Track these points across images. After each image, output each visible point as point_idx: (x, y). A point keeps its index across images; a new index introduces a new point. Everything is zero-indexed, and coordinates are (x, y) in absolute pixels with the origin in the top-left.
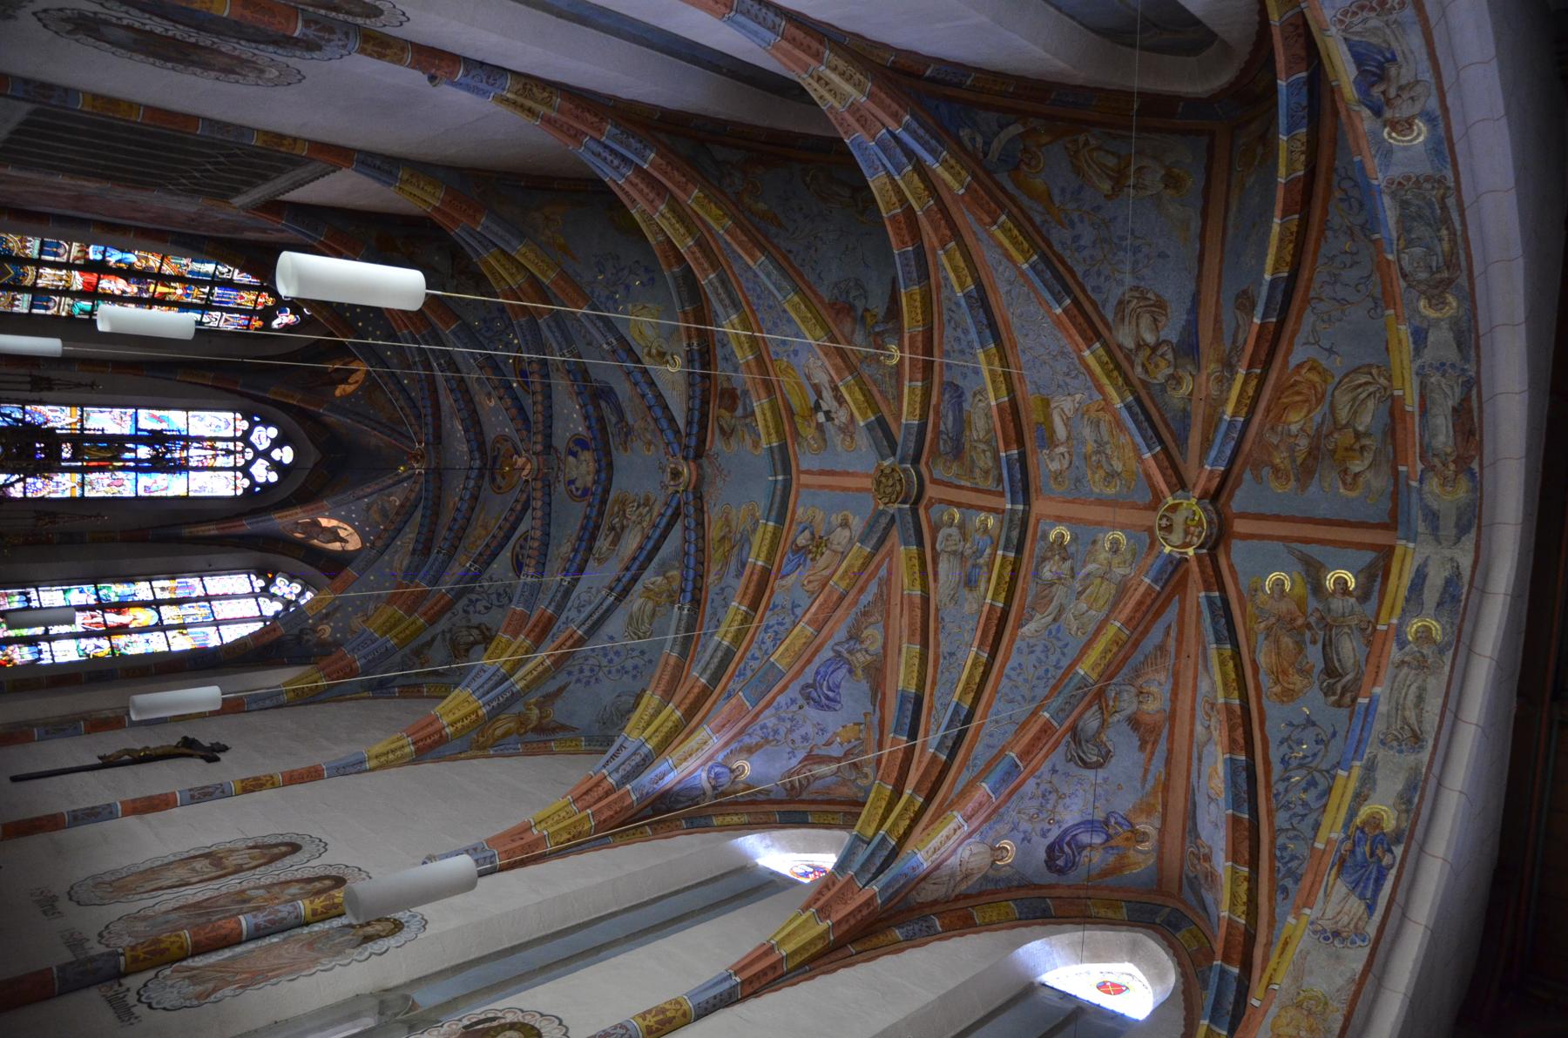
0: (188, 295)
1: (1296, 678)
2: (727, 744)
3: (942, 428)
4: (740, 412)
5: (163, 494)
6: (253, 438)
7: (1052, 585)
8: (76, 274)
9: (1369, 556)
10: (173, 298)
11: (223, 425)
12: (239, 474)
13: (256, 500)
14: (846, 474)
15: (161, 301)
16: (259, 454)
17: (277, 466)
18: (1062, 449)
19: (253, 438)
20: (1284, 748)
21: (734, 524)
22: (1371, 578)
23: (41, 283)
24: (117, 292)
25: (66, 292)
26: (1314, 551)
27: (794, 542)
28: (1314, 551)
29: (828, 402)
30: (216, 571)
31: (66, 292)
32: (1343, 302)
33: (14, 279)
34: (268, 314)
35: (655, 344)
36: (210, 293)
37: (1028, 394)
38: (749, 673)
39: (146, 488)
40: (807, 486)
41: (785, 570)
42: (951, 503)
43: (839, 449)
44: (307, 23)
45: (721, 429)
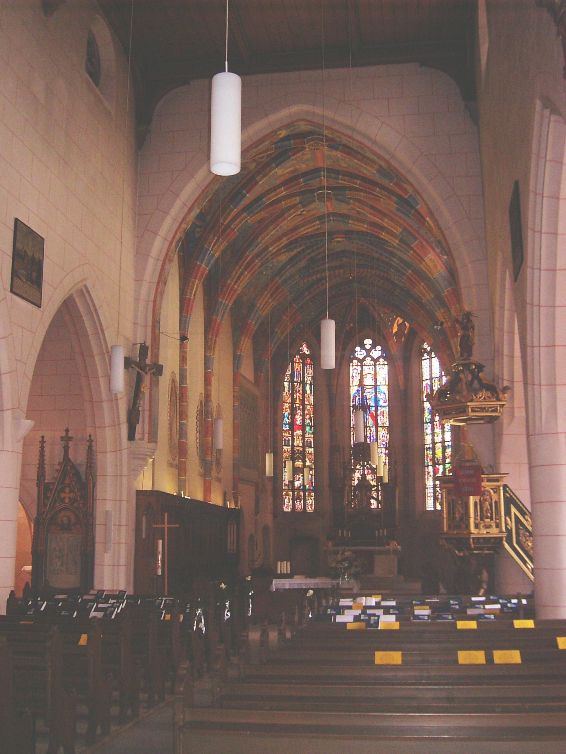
0: (299, 391)
2: (433, 249)
5: (387, 395)
6: (361, 357)
8: (295, 433)
10: (301, 396)
11: (355, 371)
12: (378, 363)
13: (387, 356)
15: (302, 401)
16: (368, 355)
17: (373, 346)
19: (361, 357)
23: (301, 445)
24: (301, 418)
25: (303, 436)
30: (420, 375)
31: (303, 436)
33: (300, 454)
34: (303, 357)
36: (297, 382)
37: (278, 182)
39: (385, 402)
44: (208, 418)
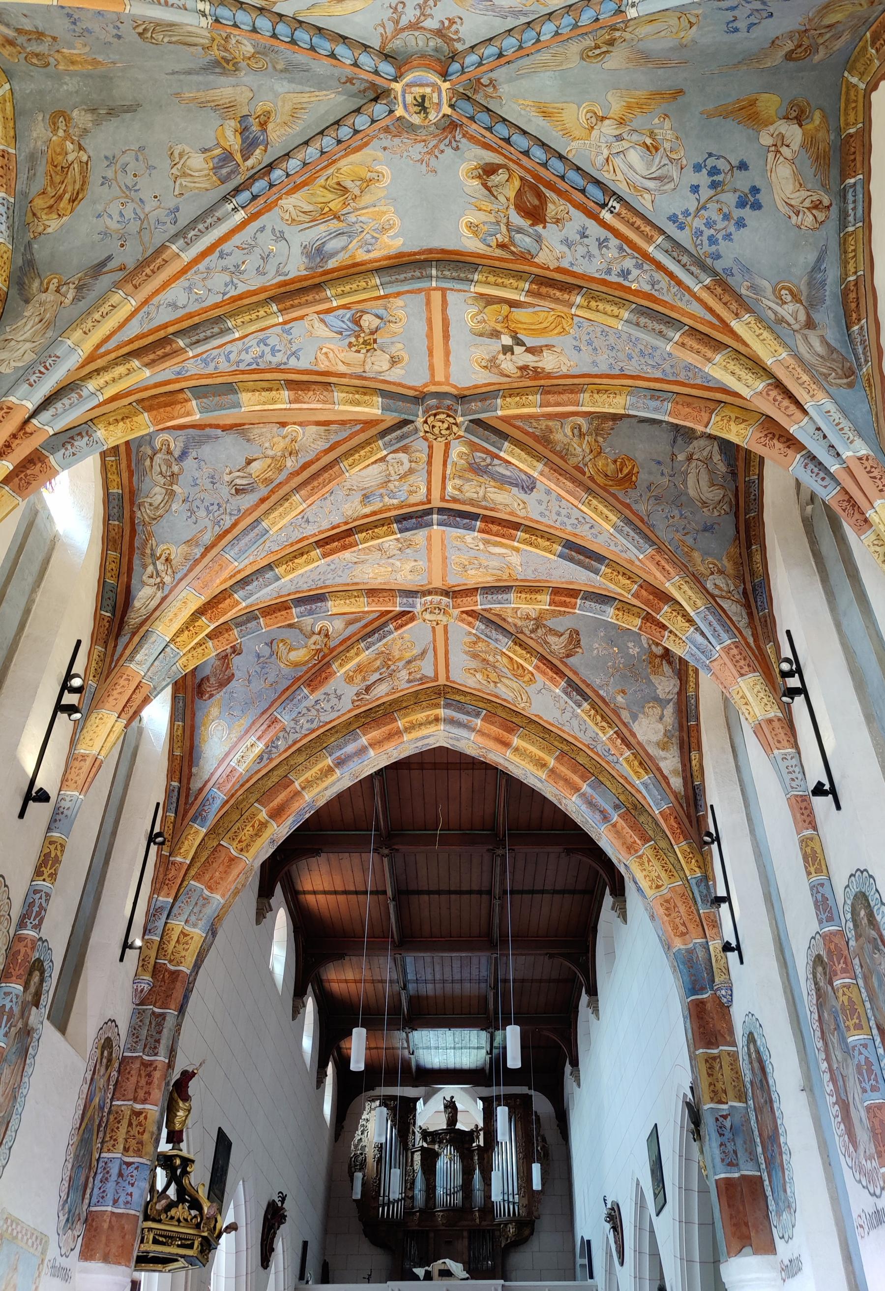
1: (359, 677)
3: (496, 462)
4: (518, 220)
7: (380, 550)
9: (432, 674)
14: (447, 353)
18: (482, 546)
20: (323, 697)
21: (366, 199)
22: (421, 679)
26: (430, 653)
27: (364, 312)
28: (430, 654)
29: (522, 357)
32: (564, 711)
35: (627, 36)
38: (212, 365)
40: (428, 303)
41: (329, 318)
42: (430, 457)
43: (473, 349)
45: (489, 170)
